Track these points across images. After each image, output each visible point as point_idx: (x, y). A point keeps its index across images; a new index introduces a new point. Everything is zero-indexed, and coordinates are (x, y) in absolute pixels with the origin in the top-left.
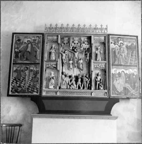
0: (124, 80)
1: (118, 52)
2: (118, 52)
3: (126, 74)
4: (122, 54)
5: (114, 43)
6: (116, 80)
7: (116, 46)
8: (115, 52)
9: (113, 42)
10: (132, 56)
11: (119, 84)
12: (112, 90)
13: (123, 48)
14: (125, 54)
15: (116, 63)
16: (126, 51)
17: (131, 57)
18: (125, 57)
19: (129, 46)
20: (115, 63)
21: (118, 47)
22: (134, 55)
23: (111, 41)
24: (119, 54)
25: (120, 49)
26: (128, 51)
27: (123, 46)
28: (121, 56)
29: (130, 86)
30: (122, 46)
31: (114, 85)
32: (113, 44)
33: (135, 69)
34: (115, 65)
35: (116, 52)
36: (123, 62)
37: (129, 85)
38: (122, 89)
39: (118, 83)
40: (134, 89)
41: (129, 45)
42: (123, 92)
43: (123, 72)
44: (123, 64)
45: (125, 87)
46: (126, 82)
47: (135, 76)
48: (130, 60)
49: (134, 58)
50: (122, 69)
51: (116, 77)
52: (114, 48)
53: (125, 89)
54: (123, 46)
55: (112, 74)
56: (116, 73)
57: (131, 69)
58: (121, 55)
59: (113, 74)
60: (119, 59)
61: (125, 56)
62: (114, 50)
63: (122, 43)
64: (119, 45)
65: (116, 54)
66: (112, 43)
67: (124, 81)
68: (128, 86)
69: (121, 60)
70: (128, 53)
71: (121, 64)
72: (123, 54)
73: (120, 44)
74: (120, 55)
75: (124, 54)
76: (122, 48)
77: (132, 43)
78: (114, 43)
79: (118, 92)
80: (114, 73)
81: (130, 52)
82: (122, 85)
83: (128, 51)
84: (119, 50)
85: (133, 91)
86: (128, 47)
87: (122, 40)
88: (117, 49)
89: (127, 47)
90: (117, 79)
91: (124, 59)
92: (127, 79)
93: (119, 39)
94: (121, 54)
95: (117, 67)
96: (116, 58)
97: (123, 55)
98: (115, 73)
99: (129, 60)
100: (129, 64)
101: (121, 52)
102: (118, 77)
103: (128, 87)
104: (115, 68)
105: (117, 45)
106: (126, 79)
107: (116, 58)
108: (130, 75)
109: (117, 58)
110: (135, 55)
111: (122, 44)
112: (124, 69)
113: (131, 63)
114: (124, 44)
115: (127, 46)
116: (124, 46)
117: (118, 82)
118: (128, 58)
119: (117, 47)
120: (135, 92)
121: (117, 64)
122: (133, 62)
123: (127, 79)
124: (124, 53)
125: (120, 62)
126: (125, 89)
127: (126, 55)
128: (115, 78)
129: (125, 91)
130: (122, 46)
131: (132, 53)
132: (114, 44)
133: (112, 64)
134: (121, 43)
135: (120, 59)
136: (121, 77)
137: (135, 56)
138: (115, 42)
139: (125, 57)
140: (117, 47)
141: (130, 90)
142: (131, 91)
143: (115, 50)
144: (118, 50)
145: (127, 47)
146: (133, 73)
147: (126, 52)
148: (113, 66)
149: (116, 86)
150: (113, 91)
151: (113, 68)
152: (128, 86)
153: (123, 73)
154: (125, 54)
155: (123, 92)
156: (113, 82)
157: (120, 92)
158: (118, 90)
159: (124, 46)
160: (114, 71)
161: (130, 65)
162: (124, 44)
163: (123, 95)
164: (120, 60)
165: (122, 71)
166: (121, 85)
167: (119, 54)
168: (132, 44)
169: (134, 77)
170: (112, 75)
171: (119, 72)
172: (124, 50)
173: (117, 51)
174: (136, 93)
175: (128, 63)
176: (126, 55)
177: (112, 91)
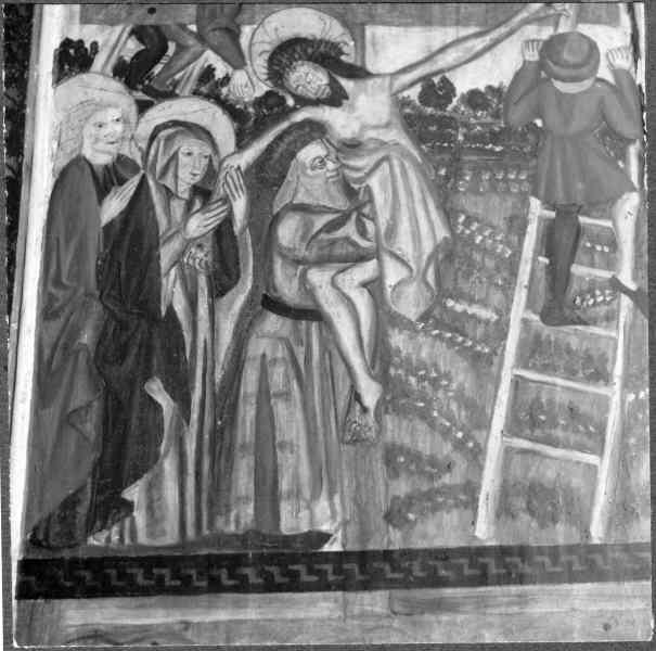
1: (223, 234)
2: (201, 257)
4: (319, 277)
5: (132, 47)
7: (161, 113)
8: (132, 245)
9: (112, 40)
10: (558, 301)
13: (353, 146)
14: (374, 287)
15: (158, 510)
17: (534, 351)
18: (381, 357)
19: (474, 99)
20: (111, 507)
21: (223, 128)
22: (616, 286)
24: (238, 298)
25: (266, 178)
26: (449, 215)
27: (325, 114)
28: (273, 323)
30: (303, 102)
32: (99, 84)
35: (166, 254)
36: (324, 477)
44: (320, 517)
48: (529, 417)
49: (618, 370)
54: (336, 98)
60: (226, 400)
61: (384, 317)
62: (114, 206)
63: (326, 56)
64: (248, 85)
65: (173, 294)
66: (74, 58)
69: (290, 422)
70: (452, 259)
71: (292, 521)
72: (343, 299)
73: (260, 64)
74: (273, 304)
75: (367, 270)
76: (311, 152)
77: (546, 33)
78: (132, 47)
81: (517, 224)
83: (468, 203)
84: (240, 206)
86: (446, 123)
88: (188, 174)
89: (430, 115)
91: (370, 393)
94: (288, 290)
96: (157, 391)
99: (484, 424)
100: (485, 531)
101: (288, 232)
105: (210, 87)
107: (157, 391)
109: (181, 393)
111: (309, 78)
113: (530, 496)
114: (358, 73)
115: (437, 90)
118: (462, 377)
121: (170, 537)
122: (605, 466)
125: (243, 480)
127: (410, 305)
130: (303, 102)
131: (561, 243)
132: (131, 74)
135: (248, 413)
137: (626, 301)
138: (154, 43)
139: (398, 339)
140: (189, 146)
144: (202, 193)
145: (430, 115)
147: (404, 244)
154: (374, 287)
159: (366, 112)
162: (358, 73)
164: (266, 419)
167: (238, 298)
168: (550, 48)
172: (356, 198)
175: (468, 495)
176: (410, 305)
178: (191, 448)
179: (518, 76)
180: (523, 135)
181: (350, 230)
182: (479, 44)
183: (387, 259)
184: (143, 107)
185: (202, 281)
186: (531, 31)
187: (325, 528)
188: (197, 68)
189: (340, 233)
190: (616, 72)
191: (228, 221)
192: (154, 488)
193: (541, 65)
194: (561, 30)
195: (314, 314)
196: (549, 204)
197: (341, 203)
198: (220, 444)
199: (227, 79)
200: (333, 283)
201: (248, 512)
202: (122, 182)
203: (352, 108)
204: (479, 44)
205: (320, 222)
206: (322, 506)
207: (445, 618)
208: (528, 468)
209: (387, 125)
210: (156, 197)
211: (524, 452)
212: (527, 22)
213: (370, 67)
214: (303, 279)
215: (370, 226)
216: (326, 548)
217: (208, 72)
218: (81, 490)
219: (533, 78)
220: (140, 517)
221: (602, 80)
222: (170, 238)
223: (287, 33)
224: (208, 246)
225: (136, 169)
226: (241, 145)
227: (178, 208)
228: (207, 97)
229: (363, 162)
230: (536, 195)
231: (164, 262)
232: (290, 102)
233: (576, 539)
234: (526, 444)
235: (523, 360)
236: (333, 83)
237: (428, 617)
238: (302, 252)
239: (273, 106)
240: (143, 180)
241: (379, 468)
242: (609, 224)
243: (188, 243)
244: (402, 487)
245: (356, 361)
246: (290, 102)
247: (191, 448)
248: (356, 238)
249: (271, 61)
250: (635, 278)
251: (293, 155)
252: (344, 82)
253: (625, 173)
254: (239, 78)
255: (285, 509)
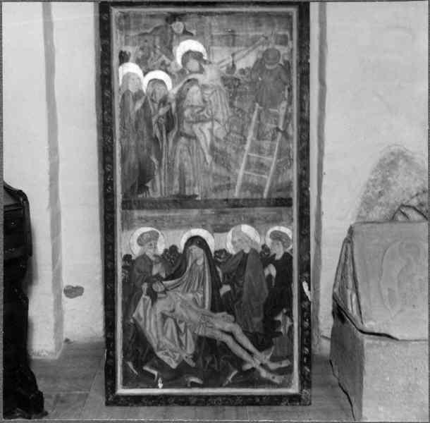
0: (200, 296)
2: (163, 121)
3: (215, 259)
6: (154, 296)
7: (151, 75)
11: (170, 323)
12: (125, 359)
13: (204, 87)
16: (223, 112)
19: (242, 71)
22: (278, 129)
23: (117, 45)
24: (173, 134)
28: (183, 140)
29: (238, 331)
30: (191, 72)
31: (136, 324)
32: (131, 68)
33: (276, 221)
34: (141, 206)
35: (154, 120)
37: (235, 322)
38: (190, 349)
39: (164, 317)
40: (261, 347)
41: (240, 65)
42: (192, 364)
43: (201, 242)
45: (208, 333)
46: (218, 305)
47: (276, 264)
50: (190, 226)
51: (151, 280)
52: (138, 95)
53: (209, 347)
54: (201, 71)
55: (127, 258)
56: (150, 253)
57: (251, 222)
58: (187, 136)
59: (134, 258)
62: (139, 105)
63: (198, 56)
66: (124, 58)
67: (200, 304)
68: (222, 326)
73: (179, 60)
75: (208, 125)
76: (195, 88)
77: (265, 48)
79: (161, 366)
80: (136, 251)
82: (186, 327)
84: (174, 105)
85: (264, 357)
87: (194, 32)
90: (158, 287)
92: (226, 289)
93: (178, 26)
95: (156, 214)
97: (197, 132)
98: (143, 257)
101: (187, 113)
102: (164, 275)
103: (231, 334)
104: (145, 221)
105: (164, 67)
106: (216, 286)
108: (243, 259)
109: (159, 158)
110: (281, 127)
111: (194, 65)
112: (204, 227)
116: (210, 76)
117: (161, 306)
119: (162, 82)
120: (273, 366)
123: (226, 289)
124: (203, 121)
126: (209, 347)
128: (145, 286)
129: (208, 360)
130: (191, 72)
133: (125, 196)
134: (188, 54)
136: (186, 276)
141: (239, 351)
142: (245, 356)
143: (145, 106)
146: (264, 246)
148: (131, 208)
149: (152, 330)
150: (130, 365)
151: (129, 225)
152: (222, 326)
153: (196, 251)
154: (211, 131)
155: (192, 364)
156: (129, 306)
157: (174, 365)
158: (160, 354)
160: (140, 241)
161: (248, 194)
163: (194, 385)
165: (193, 240)
166: (182, 326)
168: (265, 54)
169: (267, 272)
170: (124, 267)
171: (173, 249)
173: (162, 111)
174: (280, 372)
176: (221, 135)
177: (125, 366)
178: (163, 174)
179: (256, 62)
180: (255, 83)
181: (205, 112)
182: (244, 53)
183: (214, 121)
184: (145, 74)
185: (164, 128)
186: (260, 48)
187: (197, 194)
188: (160, 60)
189: (201, 114)
190: (284, 61)
191: (171, 109)
192: (154, 183)
193: (262, 59)
194: (270, 47)
195: (195, 138)
196: (261, 105)
197: (202, 104)
198: (170, 170)
199: (169, 65)
200: (200, 129)
201: (178, 189)
202: (140, 98)
203: (206, 74)
204: (244, 53)
205: (196, 110)
206: (196, 189)
207: (226, 215)
208: (248, 179)
209: (217, 80)
210: (150, 102)
211: (250, 175)
212: (259, 45)
213: (212, 60)
214: (191, 127)
215: (210, 112)
216: (197, 199)
217: (163, 63)
218: (135, 183)
219: (260, 64)
220: (150, 190)
221: (281, 65)
222: (154, 115)
223: (187, 49)
224: (165, 117)
225: (144, 95)
226: (174, 84)
227: (156, 105)
228: (163, 70)
229: (209, 92)
230: (257, 101)
231: (153, 123)
232: (188, 72)
233: (259, 196)
234: (249, 173)
235: (251, 150)
236: (200, 66)
237: (222, 215)
238: (191, 119)
239: (182, 72)
240: (146, 98)
241: (211, 180)
242: (277, 111)
243: (159, 117)
244: (217, 184)
245: (206, 151)
246: (188, 72)
247: (163, 174)
248: (206, 115)
249: (183, 59)
250: (283, 127)
251: (188, 89)
252: (204, 66)
253: (284, 95)
254: (173, 63)
255: (187, 189)
